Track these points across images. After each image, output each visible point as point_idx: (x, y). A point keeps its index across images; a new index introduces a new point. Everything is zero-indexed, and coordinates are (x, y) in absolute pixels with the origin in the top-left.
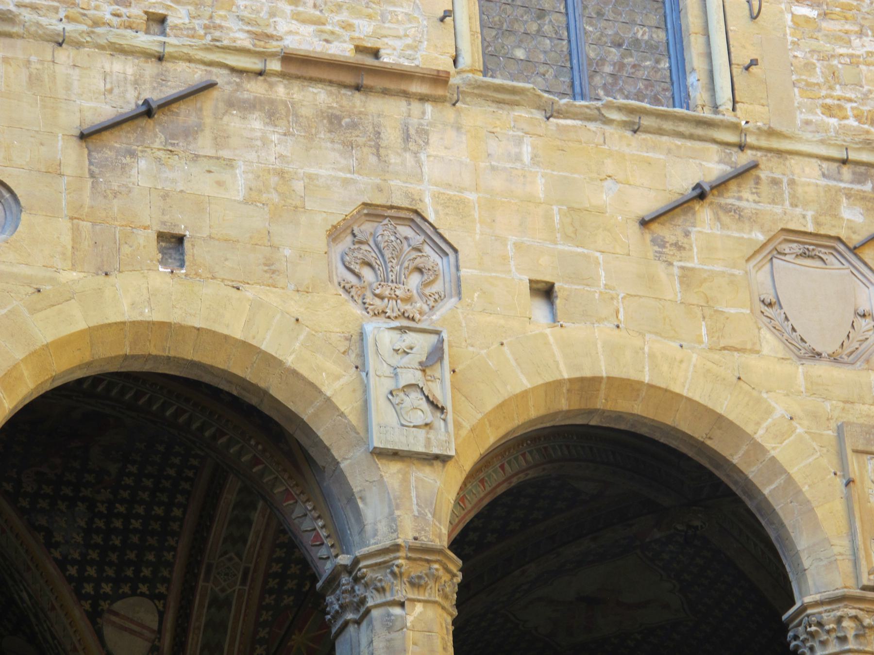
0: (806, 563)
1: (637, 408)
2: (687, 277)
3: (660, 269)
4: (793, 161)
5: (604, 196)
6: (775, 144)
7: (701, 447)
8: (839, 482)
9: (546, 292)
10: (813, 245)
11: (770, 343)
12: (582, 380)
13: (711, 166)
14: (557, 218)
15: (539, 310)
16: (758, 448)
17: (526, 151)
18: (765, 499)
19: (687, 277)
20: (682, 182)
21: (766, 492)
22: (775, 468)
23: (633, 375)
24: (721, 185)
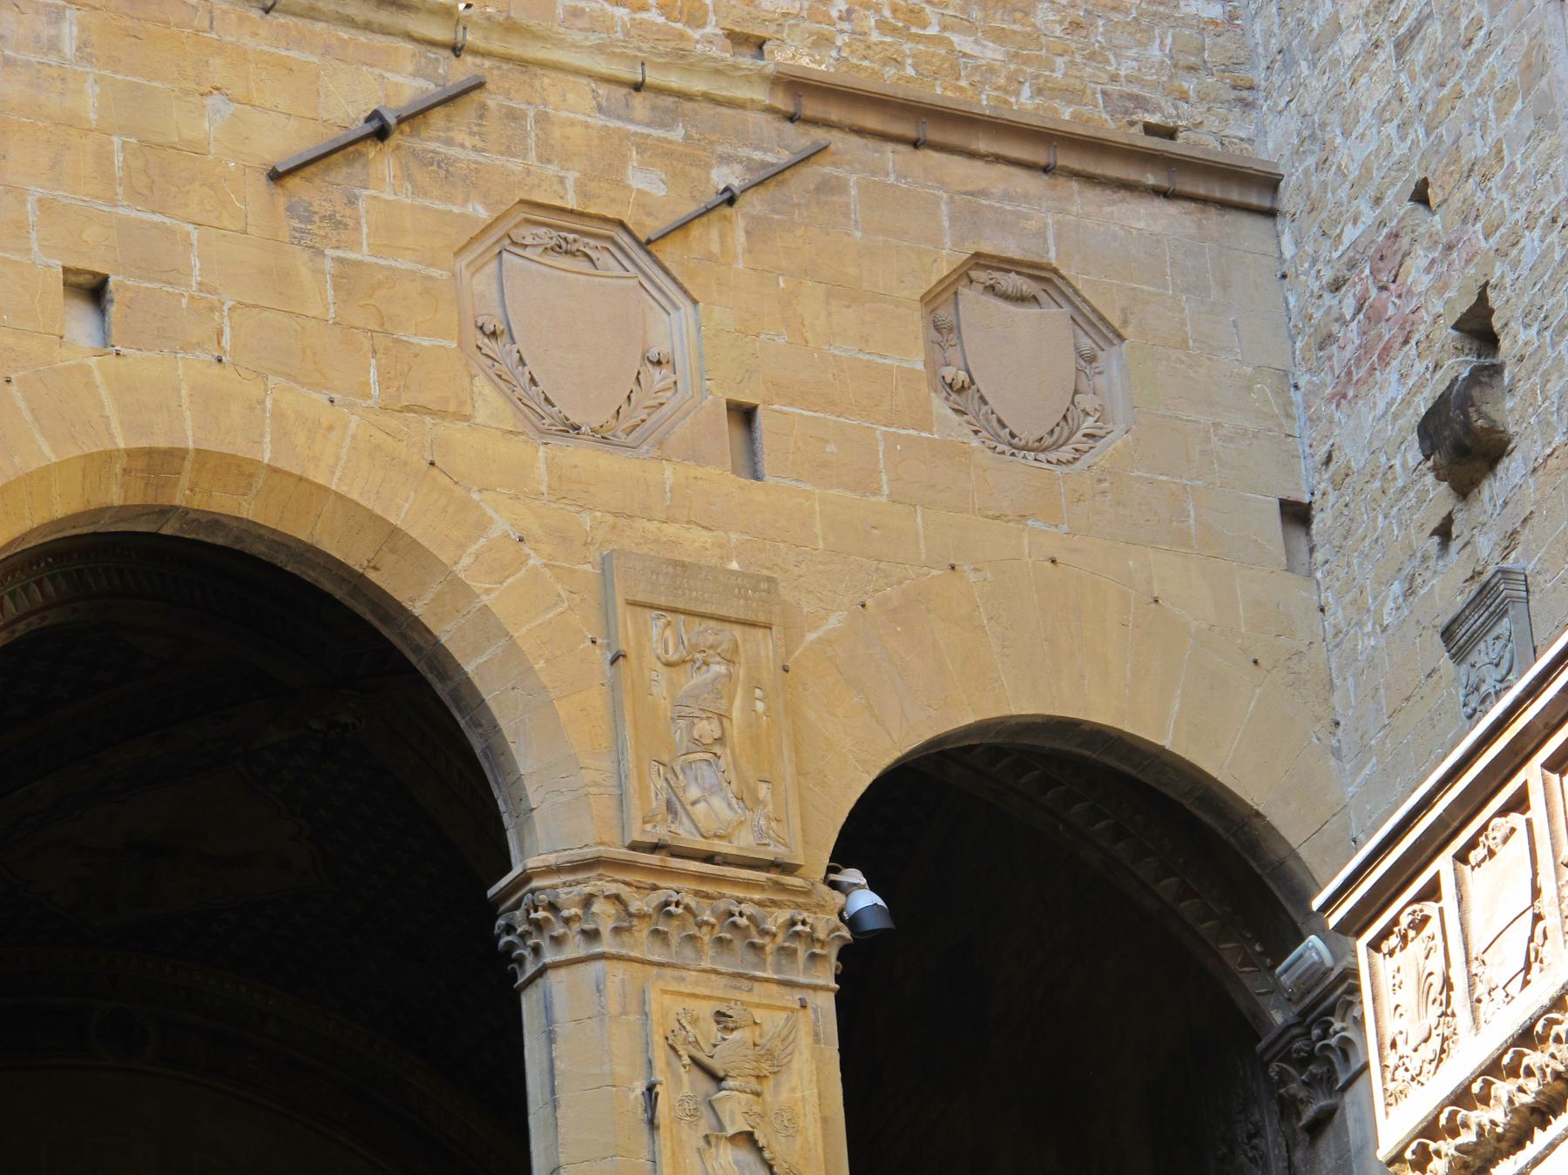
0: (534, 797)
1: (248, 508)
2: (348, 278)
3: (300, 260)
4: (546, 80)
5: (208, 123)
6: (517, 48)
7: (358, 583)
8: (602, 656)
9: (95, 292)
10: (575, 231)
11: (489, 402)
12: (150, 452)
13: (402, 82)
14: (118, 159)
15: (79, 322)
16: (459, 588)
17: (69, 34)
18: (469, 681)
19: (348, 278)
20: (347, 102)
21: (469, 668)
22: (488, 625)
23: (242, 449)
24: (417, 116)
